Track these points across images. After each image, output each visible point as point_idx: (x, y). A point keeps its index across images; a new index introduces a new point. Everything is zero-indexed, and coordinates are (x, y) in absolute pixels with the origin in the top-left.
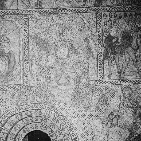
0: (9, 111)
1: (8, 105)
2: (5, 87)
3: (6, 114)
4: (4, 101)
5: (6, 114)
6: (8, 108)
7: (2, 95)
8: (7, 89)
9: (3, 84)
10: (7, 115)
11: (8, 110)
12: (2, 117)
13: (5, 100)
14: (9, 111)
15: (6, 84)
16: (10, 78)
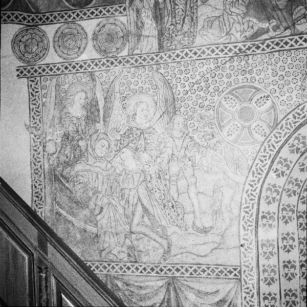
0: (301, 107)
1: (295, 92)
2: (286, 39)
3: (290, 116)
4: (283, 82)
5: (290, 116)
6: (295, 99)
7: (278, 65)
8: (292, 46)
9: (278, 32)
10: (295, 117)
11: (297, 104)
12: (280, 125)
13: (286, 78)
14: (301, 107)
15: (288, 32)
16: (299, 15)
